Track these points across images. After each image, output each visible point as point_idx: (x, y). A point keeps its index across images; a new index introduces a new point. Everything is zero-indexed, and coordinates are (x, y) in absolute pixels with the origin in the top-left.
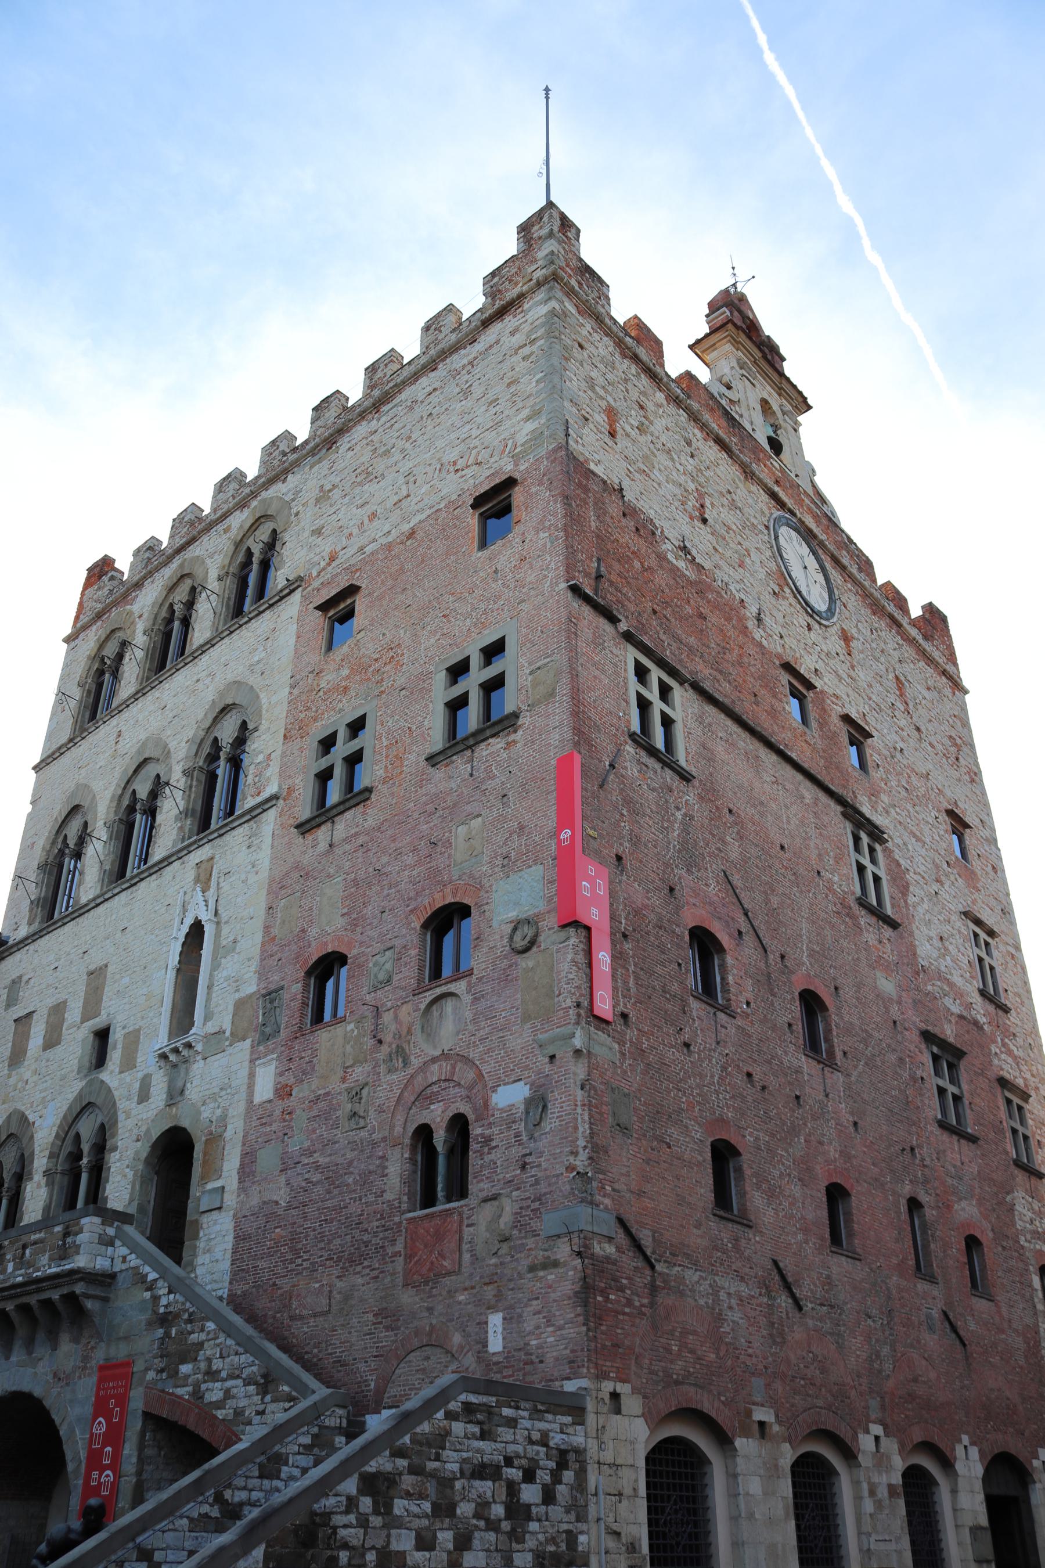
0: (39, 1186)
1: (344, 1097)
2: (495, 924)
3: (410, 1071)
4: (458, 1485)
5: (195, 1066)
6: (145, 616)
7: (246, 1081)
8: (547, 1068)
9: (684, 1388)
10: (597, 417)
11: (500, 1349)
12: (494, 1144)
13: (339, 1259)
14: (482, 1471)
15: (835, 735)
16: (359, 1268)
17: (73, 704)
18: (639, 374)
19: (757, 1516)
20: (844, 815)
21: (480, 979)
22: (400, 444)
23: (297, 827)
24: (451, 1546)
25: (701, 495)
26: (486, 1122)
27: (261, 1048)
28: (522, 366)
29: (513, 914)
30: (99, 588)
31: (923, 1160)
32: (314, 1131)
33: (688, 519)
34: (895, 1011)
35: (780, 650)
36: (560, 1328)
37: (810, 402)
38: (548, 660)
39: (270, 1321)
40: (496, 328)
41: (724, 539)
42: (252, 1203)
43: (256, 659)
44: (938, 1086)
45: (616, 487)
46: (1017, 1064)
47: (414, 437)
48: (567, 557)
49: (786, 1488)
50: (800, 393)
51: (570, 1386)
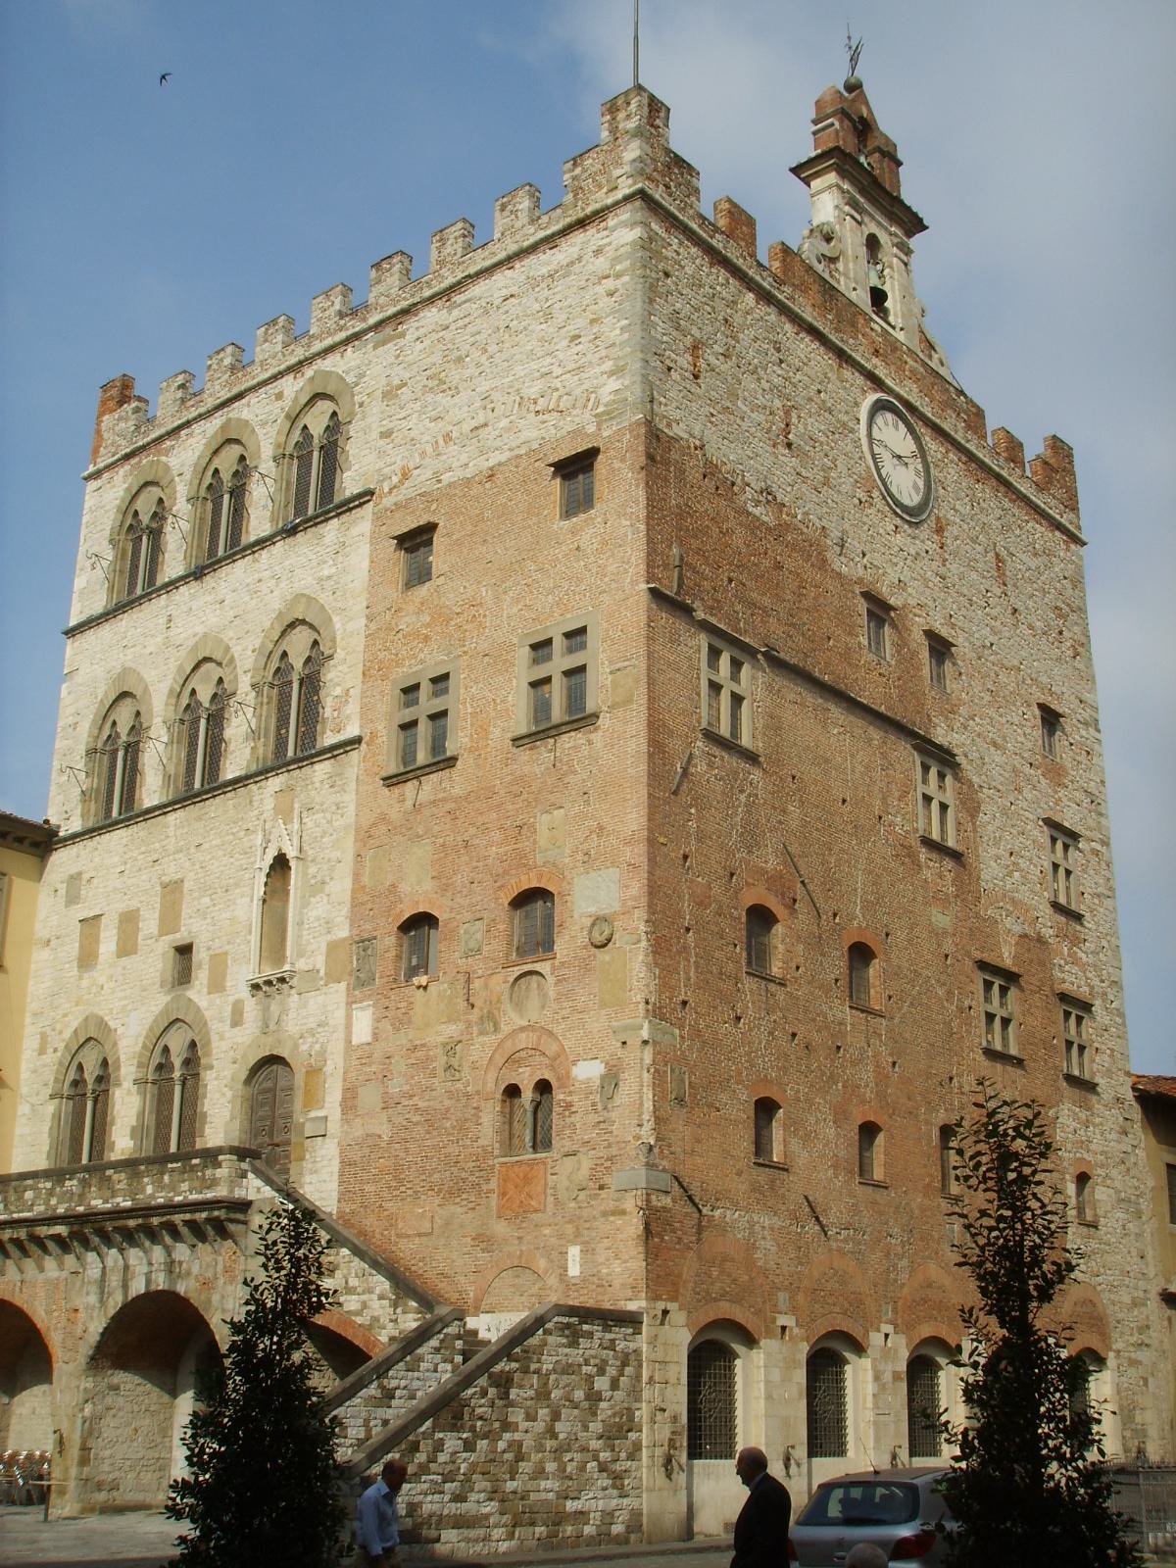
0: (129, 1092)
1: (440, 1051)
2: (576, 916)
3: (500, 1036)
4: (552, 1377)
5: (291, 999)
6: (188, 476)
7: (343, 1021)
8: (620, 1053)
9: (722, 1304)
11: (578, 1274)
12: (573, 1109)
13: (440, 1191)
14: (568, 1369)
15: (914, 654)
16: (458, 1200)
17: (105, 564)
18: (727, 280)
19: (775, 1397)
20: (915, 747)
21: (563, 963)
22: (476, 354)
23: (384, 779)
24: (548, 1419)
25: (787, 413)
26: (567, 1090)
27: (357, 992)
28: (606, 303)
29: (592, 909)
30: (120, 419)
31: (961, 1087)
32: (412, 1077)
33: (770, 449)
34: (948, 946)
36: (626, 1262)
37: (925, 223)
38: (626, 663)
39: (378, 1236)
40: (578, 238)
42: (356, 1134)
43: (326, 573)
44: (986, 1013)
45: (698, 443)
46: (1084, 972)
47: (492, 348)
48: (649, 554)
49: (801, 1376)
50: (915, 215)
51: (632, 1306)
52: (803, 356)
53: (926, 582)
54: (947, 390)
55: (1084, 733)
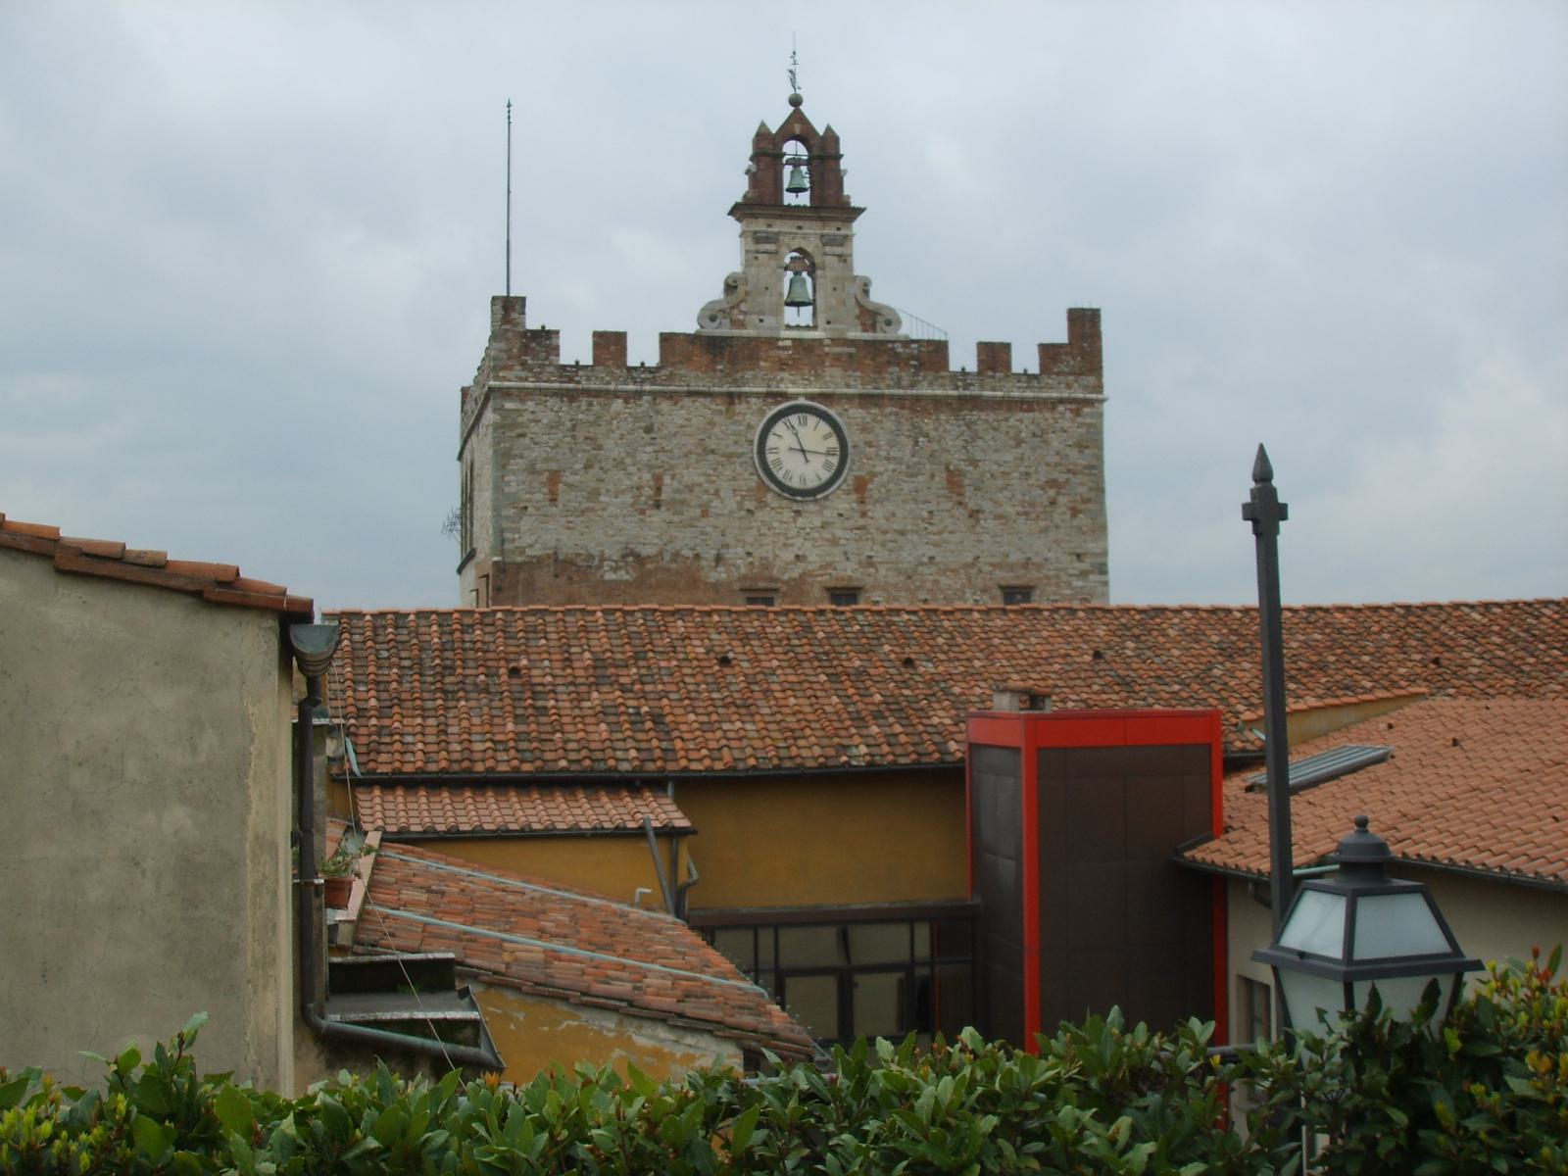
10: (539, 496)
18: (590, 404)
25: (658, 479)
35: (743, 571)
41: (683, 502)
52: (681, 422)
53: (834, 542)
54: (893, 349)
55: (1080, 583)
